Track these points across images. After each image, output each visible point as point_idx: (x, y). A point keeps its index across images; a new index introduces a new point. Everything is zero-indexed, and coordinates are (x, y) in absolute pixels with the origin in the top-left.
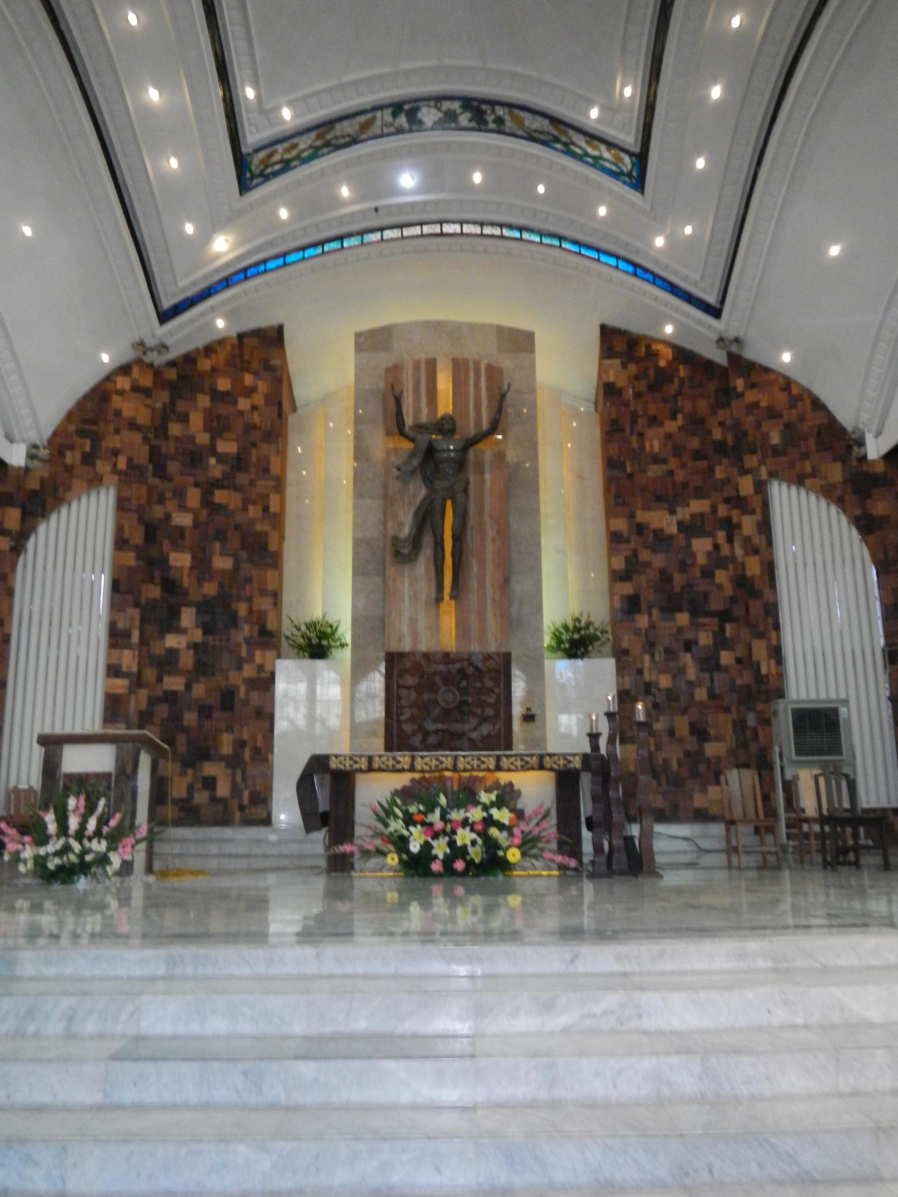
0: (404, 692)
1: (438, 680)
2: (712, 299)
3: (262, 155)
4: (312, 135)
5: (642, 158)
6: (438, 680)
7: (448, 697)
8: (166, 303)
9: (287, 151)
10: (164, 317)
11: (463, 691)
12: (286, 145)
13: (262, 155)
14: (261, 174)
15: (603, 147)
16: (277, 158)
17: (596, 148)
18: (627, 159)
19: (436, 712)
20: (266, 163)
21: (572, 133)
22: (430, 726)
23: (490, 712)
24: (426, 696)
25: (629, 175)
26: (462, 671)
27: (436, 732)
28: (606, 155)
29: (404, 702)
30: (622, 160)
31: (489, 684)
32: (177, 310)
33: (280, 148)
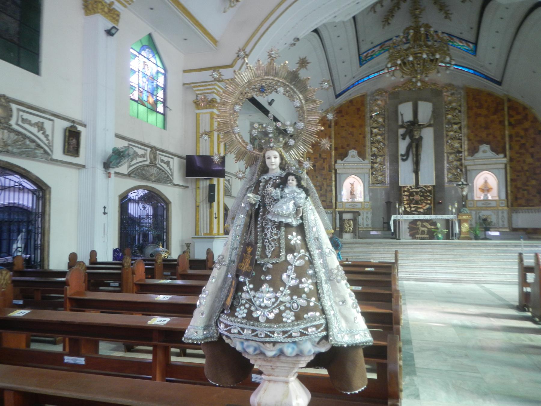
0: (404, 197)
1: (414, 193)
2: (498, 80)
3: (365, 54)
4: (378, 47)
5: (476, 44)
6: (414, 193)
7: (417, 197)
8: (338, 93)
9: (372, 52)
10: (337, 96)
11: (421, 196)
12: (371, 51)
13: (365, 54)
14: (365, 60)
15: (464, 42)
16: (369, 55)
17: (462, 43)
18: (471, 45)
19: (414, 202)
20: (366, 57)
21: (454, 38)
22: (412, 206)
23: (429, 202)
24: (411, 198)
25: (471, 50)
26: (421, 191)
27: (414, 207)
28: (465, 45)
29: (405, 199)
30: (469, 46)
31: (428, 194)
32: (340, 95)
33: (370, 52)
